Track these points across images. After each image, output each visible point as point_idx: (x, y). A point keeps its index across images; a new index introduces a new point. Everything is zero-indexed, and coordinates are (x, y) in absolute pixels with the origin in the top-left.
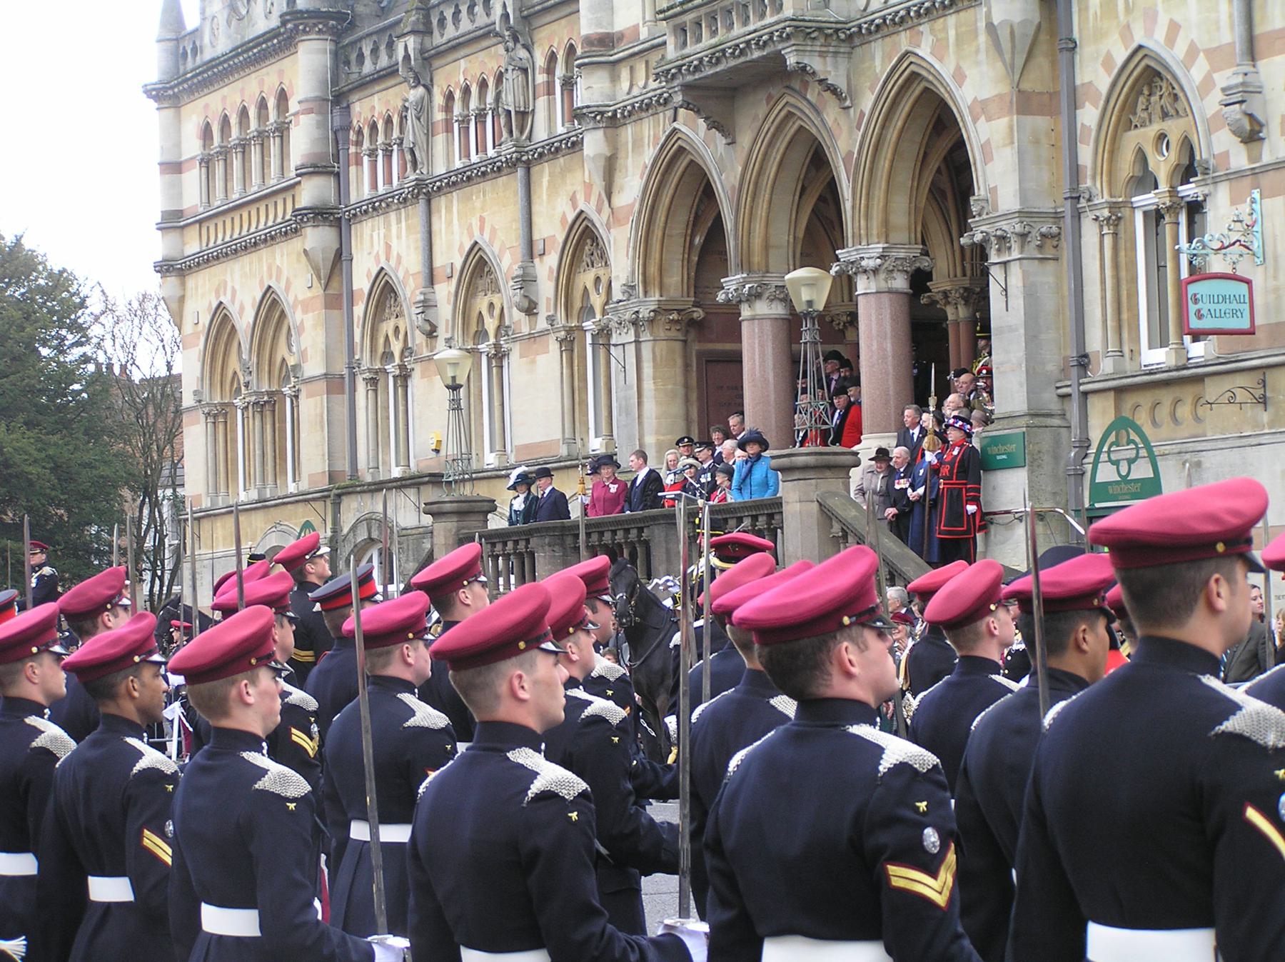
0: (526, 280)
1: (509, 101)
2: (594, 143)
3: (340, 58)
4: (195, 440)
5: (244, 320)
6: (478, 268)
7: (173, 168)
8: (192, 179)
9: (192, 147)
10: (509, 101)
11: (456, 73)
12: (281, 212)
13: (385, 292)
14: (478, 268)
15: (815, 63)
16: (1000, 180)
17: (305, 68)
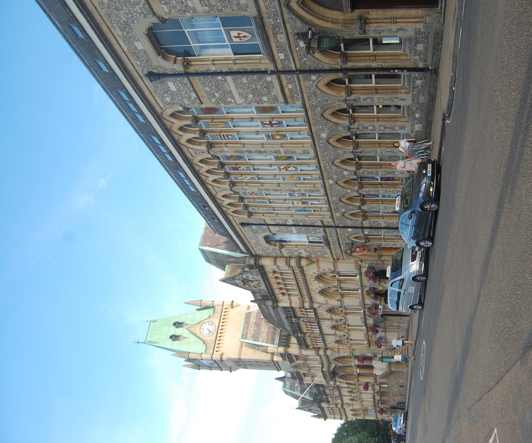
0: (352, 389)
1: (332, 388)
2: (338, 384)
3: (324, 401)
4: (368, 418)
5: (354, 413)
6: (350, 392)
7: (335, 418)
8: (336, 416)
9: (333, 416)
10: (332, 388)
11: (327, 392)
12: (342, 410)
13: (352, 400)
14: (350, 392)
15: (332, 368)
16: (346, 355)
17: (324, 405)
